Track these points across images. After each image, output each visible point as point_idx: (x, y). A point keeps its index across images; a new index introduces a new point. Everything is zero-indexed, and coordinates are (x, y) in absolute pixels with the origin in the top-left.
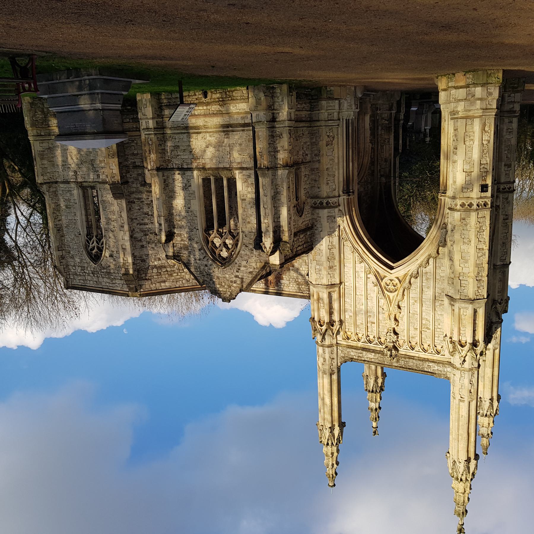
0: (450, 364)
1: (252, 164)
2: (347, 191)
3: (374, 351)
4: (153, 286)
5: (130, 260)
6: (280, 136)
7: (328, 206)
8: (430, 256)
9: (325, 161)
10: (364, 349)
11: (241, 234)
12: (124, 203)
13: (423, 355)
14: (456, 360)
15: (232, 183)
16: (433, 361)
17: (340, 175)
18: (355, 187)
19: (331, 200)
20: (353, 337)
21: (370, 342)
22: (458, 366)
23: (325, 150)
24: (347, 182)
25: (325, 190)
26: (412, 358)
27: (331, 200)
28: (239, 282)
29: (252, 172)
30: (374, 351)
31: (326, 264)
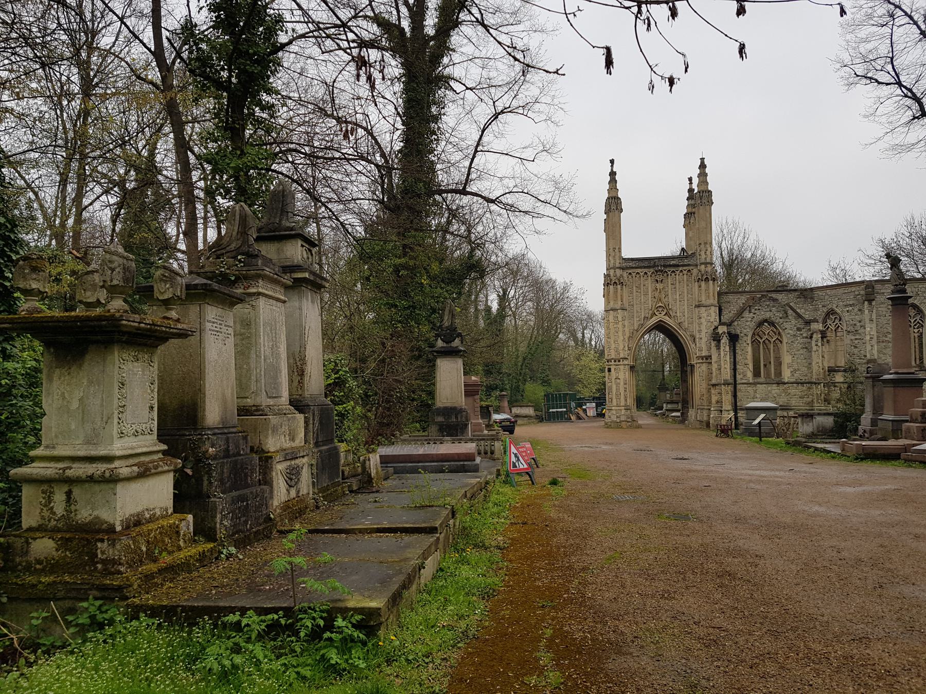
0: (623, 269)
1: (738, 387)
2: (692, 366)
3: (670, 266)
4: (853, 289)
5: (866, 312)
6: (717, 402)
7: (702, 358)
8: (637, 331)
9: (704, 385)
10: (678, 266)
11: (749, 342)
12: (868, 356)
13: (639, 270)
14: (619, 272)
15: (757, 373)
16: (633, 268)
17: (696, 374)
18: (689, 369)
19: (701, 361)
20: (685, 272)
21: (673, 272)
22: (617, 270)
23: (704, 391)
24: (692, 371)
25: (704, 367)
26: (645, 267)
27: (701, 361)
28: (753, 311)
29: (739, 381)
30: (670, 266)
31: (703, 320)
